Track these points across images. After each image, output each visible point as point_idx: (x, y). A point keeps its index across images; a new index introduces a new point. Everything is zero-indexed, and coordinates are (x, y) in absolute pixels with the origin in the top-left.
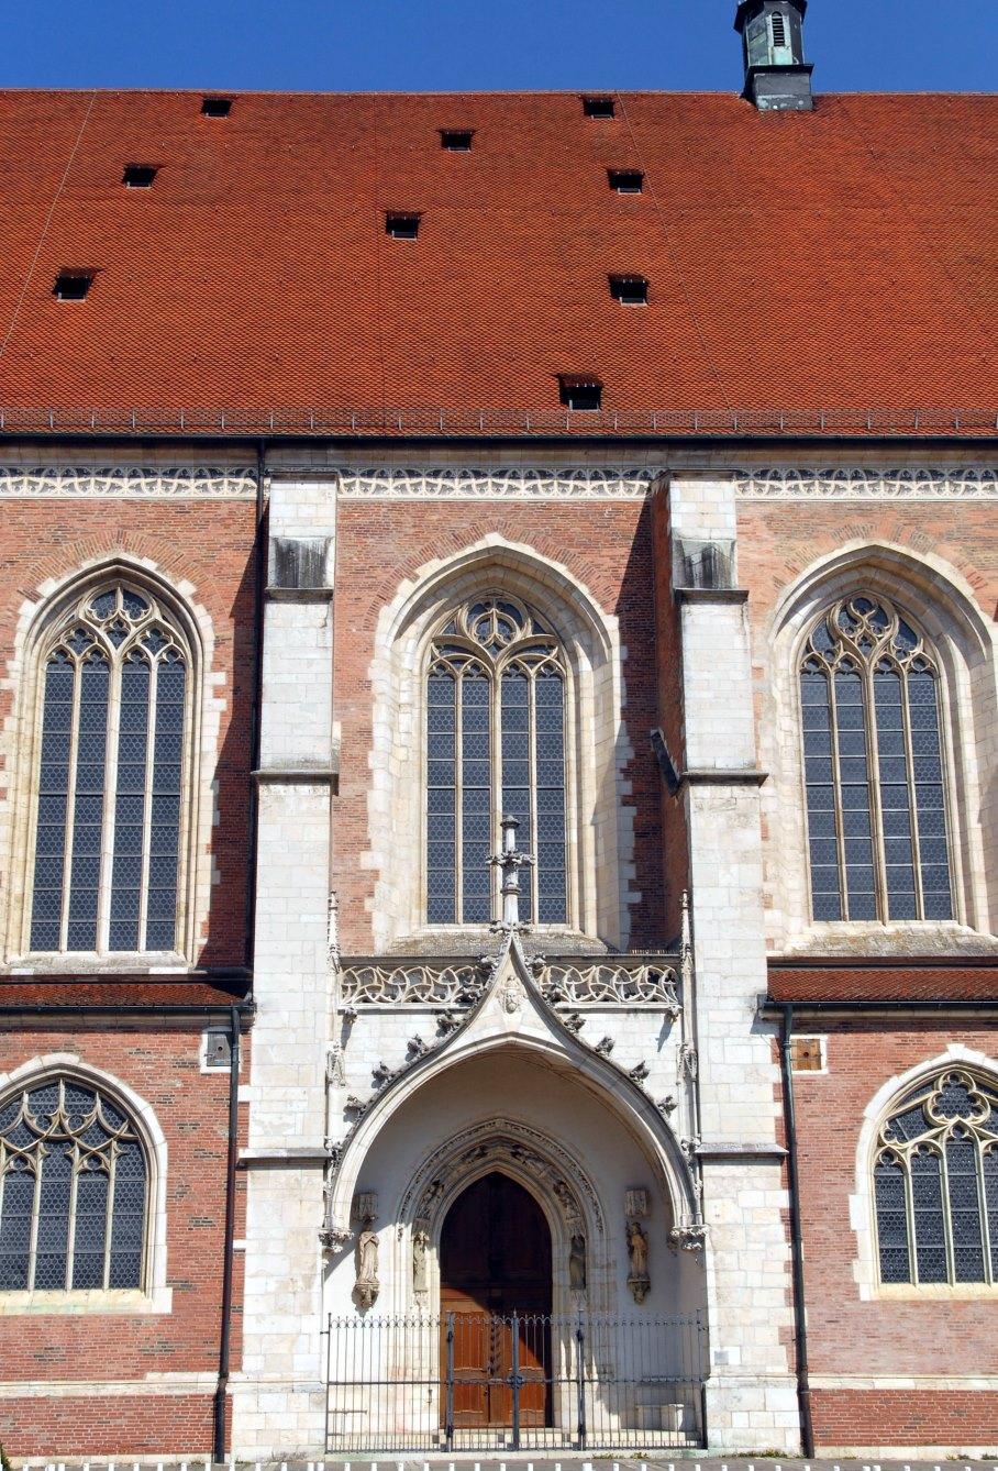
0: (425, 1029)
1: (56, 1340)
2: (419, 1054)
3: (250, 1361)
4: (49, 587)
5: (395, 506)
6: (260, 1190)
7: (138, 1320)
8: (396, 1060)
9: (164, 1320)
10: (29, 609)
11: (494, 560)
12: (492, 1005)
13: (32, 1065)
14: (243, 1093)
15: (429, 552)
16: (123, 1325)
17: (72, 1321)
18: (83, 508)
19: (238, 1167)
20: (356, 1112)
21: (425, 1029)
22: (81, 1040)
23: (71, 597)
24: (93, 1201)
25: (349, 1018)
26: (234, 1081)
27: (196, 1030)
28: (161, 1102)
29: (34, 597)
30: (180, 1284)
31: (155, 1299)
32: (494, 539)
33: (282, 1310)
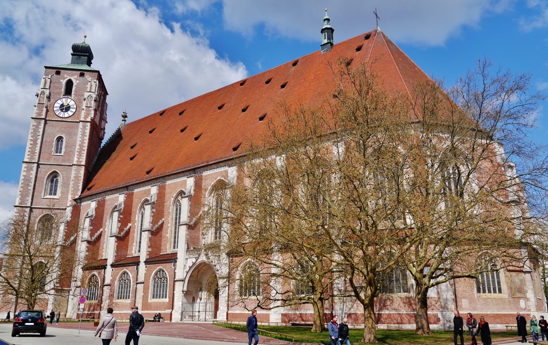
0: (194, 260)
1: (159, 305)
2: (194, 264)
3: (175, 308)
4: (174, 196)
5: (209, 175)
6: (177, 283)
7: (165, 302)
8: (191, 265)
9: (168, 303)
10: (173, 199)
11: (220, 180)
12: (201, 257)
13: (158, 268)
14: (176, 271)
15: (212, 182)
16: (164, 303)
17: (160, 303)
18: (178, 183)
19: (175, 281)
20: (187, 273)
21: (194, 260)
22: (162, 265)
23: (177, 196)
24: (164, 287)
25: (187, 259)
26: (175, 269)
27: (172, 262)
28: (169, 273)
29: (173, 197)
30: (169, 298)
31: (167, 300)
32: (219, 178)
33: (178, 301)
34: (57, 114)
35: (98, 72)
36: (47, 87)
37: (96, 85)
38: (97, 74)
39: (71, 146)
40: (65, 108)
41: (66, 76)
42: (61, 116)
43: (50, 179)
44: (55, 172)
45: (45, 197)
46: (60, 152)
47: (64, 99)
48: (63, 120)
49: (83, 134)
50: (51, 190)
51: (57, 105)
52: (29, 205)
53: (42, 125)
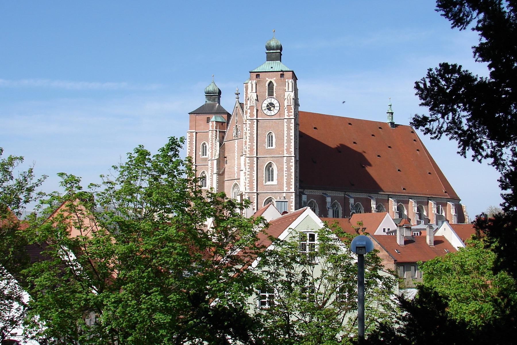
34: (265, 113)
35: (293, 72)
36: (254, 91)
37: (292, 83)
38: (291, 72)
39: (280, 139)
40: (270, 106)
41: (267, 79)
42: (269, 115)
43: (267, 168)
44: (271, 162)
45: (266, 184)
46: (272, 146)
47: (269, 99)
48: (271, 119)
49: (289, 129)
50: (269, 177)
51: (264, 105)
52: (255, 191)
53: (255, 123)
